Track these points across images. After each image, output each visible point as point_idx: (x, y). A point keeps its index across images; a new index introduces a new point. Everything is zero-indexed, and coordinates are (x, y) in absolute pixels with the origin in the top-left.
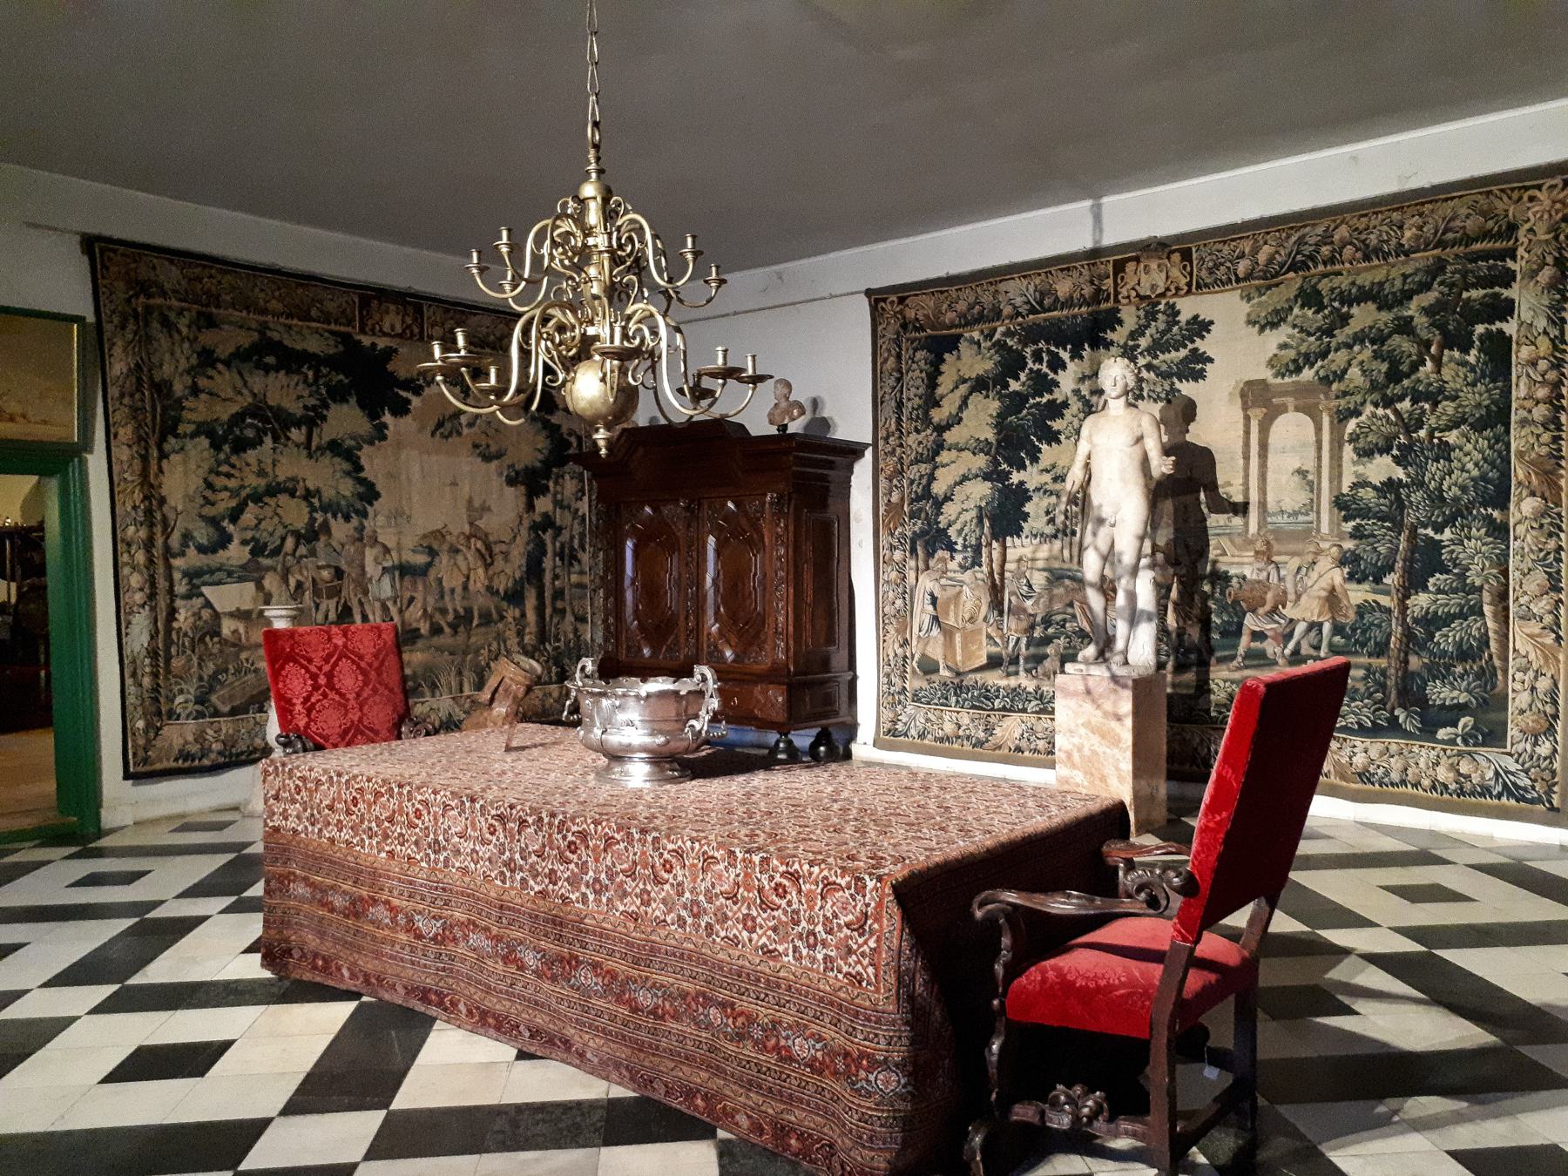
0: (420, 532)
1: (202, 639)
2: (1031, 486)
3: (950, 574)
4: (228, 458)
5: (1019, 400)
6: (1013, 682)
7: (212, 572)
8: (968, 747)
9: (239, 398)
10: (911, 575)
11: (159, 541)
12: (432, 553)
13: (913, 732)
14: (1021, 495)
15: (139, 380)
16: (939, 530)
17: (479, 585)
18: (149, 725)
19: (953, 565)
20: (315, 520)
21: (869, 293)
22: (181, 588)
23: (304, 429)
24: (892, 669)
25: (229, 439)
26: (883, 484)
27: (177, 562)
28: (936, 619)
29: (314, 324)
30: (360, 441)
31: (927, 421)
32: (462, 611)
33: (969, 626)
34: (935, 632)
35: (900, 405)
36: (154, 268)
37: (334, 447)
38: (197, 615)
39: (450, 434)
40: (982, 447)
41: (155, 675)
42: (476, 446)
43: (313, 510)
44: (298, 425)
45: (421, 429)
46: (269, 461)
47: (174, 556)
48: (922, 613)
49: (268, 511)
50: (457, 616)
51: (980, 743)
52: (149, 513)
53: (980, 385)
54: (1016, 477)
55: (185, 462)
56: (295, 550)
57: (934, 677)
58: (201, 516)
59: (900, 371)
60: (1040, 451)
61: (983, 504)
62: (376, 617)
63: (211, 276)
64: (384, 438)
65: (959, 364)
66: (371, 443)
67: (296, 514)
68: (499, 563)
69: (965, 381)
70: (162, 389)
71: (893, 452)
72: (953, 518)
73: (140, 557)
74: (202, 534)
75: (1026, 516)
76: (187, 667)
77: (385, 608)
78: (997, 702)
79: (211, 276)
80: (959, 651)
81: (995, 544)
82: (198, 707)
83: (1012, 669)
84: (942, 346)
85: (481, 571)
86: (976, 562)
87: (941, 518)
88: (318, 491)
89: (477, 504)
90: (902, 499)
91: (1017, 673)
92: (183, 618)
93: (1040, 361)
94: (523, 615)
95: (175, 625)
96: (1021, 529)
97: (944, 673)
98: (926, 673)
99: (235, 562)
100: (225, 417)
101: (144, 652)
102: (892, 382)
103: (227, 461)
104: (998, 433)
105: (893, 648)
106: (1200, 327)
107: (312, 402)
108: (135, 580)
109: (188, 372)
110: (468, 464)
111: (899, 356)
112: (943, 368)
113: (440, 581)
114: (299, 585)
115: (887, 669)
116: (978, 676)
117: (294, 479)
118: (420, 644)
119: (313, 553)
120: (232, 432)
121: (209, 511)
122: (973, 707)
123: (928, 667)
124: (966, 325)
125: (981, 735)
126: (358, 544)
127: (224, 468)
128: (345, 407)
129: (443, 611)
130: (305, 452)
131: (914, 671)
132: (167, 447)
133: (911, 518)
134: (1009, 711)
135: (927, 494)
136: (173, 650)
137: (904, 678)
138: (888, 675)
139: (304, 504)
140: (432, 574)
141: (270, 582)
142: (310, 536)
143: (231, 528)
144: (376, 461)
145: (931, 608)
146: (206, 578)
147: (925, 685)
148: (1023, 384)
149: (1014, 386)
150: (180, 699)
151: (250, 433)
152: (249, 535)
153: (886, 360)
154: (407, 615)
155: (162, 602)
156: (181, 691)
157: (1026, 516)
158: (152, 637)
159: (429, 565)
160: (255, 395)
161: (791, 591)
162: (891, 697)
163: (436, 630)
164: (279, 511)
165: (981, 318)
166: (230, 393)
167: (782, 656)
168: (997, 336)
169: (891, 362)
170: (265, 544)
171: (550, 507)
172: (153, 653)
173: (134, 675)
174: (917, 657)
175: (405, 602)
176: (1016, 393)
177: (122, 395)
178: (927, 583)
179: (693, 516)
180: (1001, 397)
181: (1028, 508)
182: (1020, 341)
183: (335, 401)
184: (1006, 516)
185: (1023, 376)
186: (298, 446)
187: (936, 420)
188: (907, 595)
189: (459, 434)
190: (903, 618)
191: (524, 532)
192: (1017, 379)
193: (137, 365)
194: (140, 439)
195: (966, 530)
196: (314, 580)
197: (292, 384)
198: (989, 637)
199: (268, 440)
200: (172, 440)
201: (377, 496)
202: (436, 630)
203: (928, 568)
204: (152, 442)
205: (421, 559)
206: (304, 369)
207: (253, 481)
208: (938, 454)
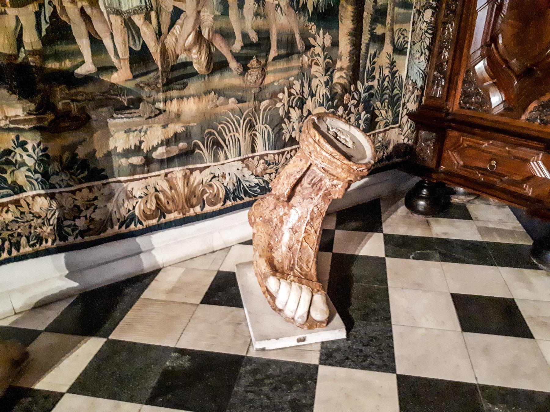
32: (254, 37)
50: (247, 44)
94: (335, 44)
118: (194, 86)
129: (227, 35)
154: (170, 41)
175: (166, 19)
202: (218, 65)
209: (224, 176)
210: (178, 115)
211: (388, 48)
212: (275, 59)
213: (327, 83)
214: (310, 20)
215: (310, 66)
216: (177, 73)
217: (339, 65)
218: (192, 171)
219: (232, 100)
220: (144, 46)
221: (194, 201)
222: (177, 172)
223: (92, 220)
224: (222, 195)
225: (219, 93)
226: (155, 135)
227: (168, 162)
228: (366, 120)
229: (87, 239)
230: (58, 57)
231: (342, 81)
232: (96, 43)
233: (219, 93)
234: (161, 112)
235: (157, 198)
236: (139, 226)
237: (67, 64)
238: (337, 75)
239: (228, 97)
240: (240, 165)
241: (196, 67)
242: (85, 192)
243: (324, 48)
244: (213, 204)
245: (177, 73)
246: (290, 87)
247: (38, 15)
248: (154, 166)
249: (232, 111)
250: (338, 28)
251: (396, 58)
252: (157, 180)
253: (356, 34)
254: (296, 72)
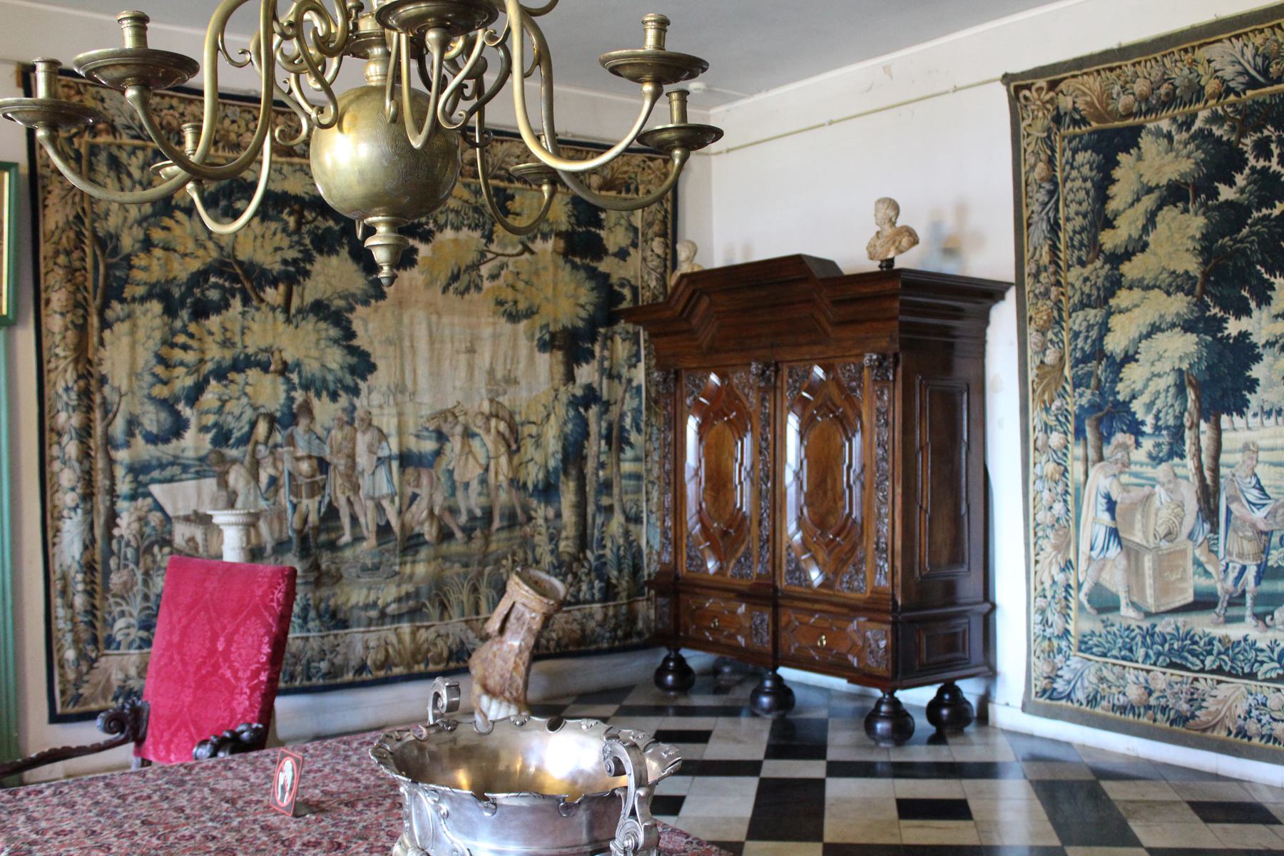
0: (426, 411)
1: (148, 550)
2: (1259, 338)
3: (1133, 468)
4: (185, 326)
5: (1233, 215)
6: (1234, 632)
7: (162, 466)
8: (1162, 722)
9: (201, 252)
10: (1077, 470)
11: (98, 429)
12: (441, 437)
13: (1080, 695)
14: (1245, 351)
15: (79, 235)
16: (1117, 404)
17: (501, 478)
18: (81, 655)
19: (1139, 455)
20: (291, 400)
21: (1007, 79)
22: (124, 487)
23: (282, 288)
24: (1051, 602)
25: (188, 302)
26: (1033, 338)
27: (122, 455)
28: (1114, 533)
29: (296, 160)
30: (353, 301)
31: (1095, 247)
32: (478, 513)
33: (1164, 544)
34: (1114, 551)
35: (1054, 228)
36: (102, 100)
37: (319, 309)
38: (142, 520)
39: (467, 289)
40: (1179, 283)
41: (90, 593)
42: (500, 303)
43: (291, 387)
44: (274, 283)
45: (430, 284)
46: (237, 329)
47: (116, 447)
48: (1094, 523)
49: (234, 390)
50: (472, 518)
51: (1182, 719)
52: (85, 394)
53: (1175, 194)
54: (1234, 327)
55: (133, 332)
56: (268, 438)
57: (1111, 617)
58: (150, 397)
59: (1053, 180)
60: (1271, 287)
61: (1185, 366)
62: (368, 521)
63: (172, 107)
64: (381, 295)
65: (1142, 167)
66: (366, 303)
67: (269, 392)
68: (529, 449)
69: (1150, 190)
70: (107, 244)
71: (1046, 294)
72: (1138, 386)
73: (72, 448)
74: (152, 419)
75: (1252, 384)
76: (128, 586)
77: (380, 508)
78: (1209, 660)
79: (172, 107)
80: (1149, 581)
81: (1204, 426)
82: (143, 634)
83: (1234, 611)
84: (1113, 143)
85: (504, 460)
86: (1176, 451)
87: (1120, 387)
88: (298, 365)
89: (499, 374)
90: (1062, 359)
91: (1241, 619)
92: (126, 525)
93: (1268, 156)
94: (558, 515)
95: (116, 532)
96: (1246, 403)
97: (1127, 612)
98: (1101, 610)
99: (190, 454)
100: (183, 276)
101: (76, 566)
102: (1042, 196)
103: (184, 330)
104: (1205, 263)
105: (1050, 571)
107: (292, 254)
108: (67, 477)
109: (140, 223)
110: (490, 326)
111: (1051, 161)
112: (1117, 173)
113: (451, 472)
114: (273, 481)
115: (1041, 602)
116: (1180, 619)
117: (269, 350)
118: (424, 553)
119: (291, 441)
120: (192, 294)
121: (161, 391)
122: (1172, 665)
123: (1104, 604)
124: (1149, 111)
125: (1185, 707)
126: (347, 429)
127: (181, 339)
128: (334, 260)
130: (281, 317)
131: (1081, 608)
132: (110, 314)
133: (1075, 386)
134: (1229, 674)
135: (1098, 353)
136: (113, 563)
137: (1066, 617)
138: (1043, 611)
139: (280, 380)
140: (443, 464)
141: (237, 478)
142: (286, 419)
143: (187, 412)
144: (371, 326)
145: (1106, 517)
146: (156, 474)
147: (1099, 628)
148: (1242, 191)
149: (1226, 193)
150: (120, 623)
151: (214, 295)
152: (210, 420)
153: (1033, 167)
154: (408, 516)
155: (101, 502)
156: (122, 614)
157: (1252, 384)
158: (86, 547)
159: (438, 453)
160: (221, 248)
161: (899, 490)
162: (1048, 644)
163: (445, 535)
164: (249, 389)
165: (1170, 101)
166: (191, 246)
167: (885, 583)
168: (1198, 124)
169: (1041, 170)
170: (230, 432)
171: (597, 377)
172: (89, 567)
173: (64, 593)
174: (1085, 589)
175: (407, 501)
176: (1228, 203)
177: (57, 253)
178: (1100, 481)
179: (769, 388)
180: (1207, 211)
181: (1257, 371)
182: (1233, 129)
183: (321, 252)
185: (1240, 180)
186: (273, 309)
187: (1108, 246)
188: (1072, 497)
189: (479, 288)
190: (1066, 530)
191: (561, 410)
192: (1231, 183)
193: (78, 217)
194: (77, 305)
195: (1159, 404)
196: (290, 474)
197: (268, 234)
198: (1198, 563)
199: (237, 303)
200: (116, 305)
201: (372, 368)
203: (1101, 459)
204: (93, 310)
205: (429, 446)
206: (285, 216)
207: (215, 353)
208: (1113, 295)
209: (447, 636)
210: (411, 577)
211: (618, 519)
212: (498, 530)
213: (552, 552)
214: (531, 495)
215: (533, 536)
216: (412, 542)
217: (564, 534)
218: (419, 628)
219: (457, 566)
220: (388, 523)
221: (419, 657)
222: (406, 627)
223: (333, 664)
224: (445, 654)
225: (445, 558)
226: (388, 594)
227: (398, 618)
228: (601, 589)
229: (328, 682)
230: (328, 530)
231: (570, 550)
232: (354, 520)
233: (445, 558)
234: (396, 573)
235: (387, 651)
236: (370, 676)
237: (333, 536)
238: (562, 545)
239: (453, 563)
240: (464, 626)
241: (427, 537)
242: (331, 638)
243: (546, 520)
244: (437, 663)
245: (412, 542)
246: (514, 554)
247: (320, 503)
248: (388, 620)
249: (458, 575)
250: (560, 502)
251: (632, 527)
252: (387, 632)
253: (581, 506)
254: (518, 541)
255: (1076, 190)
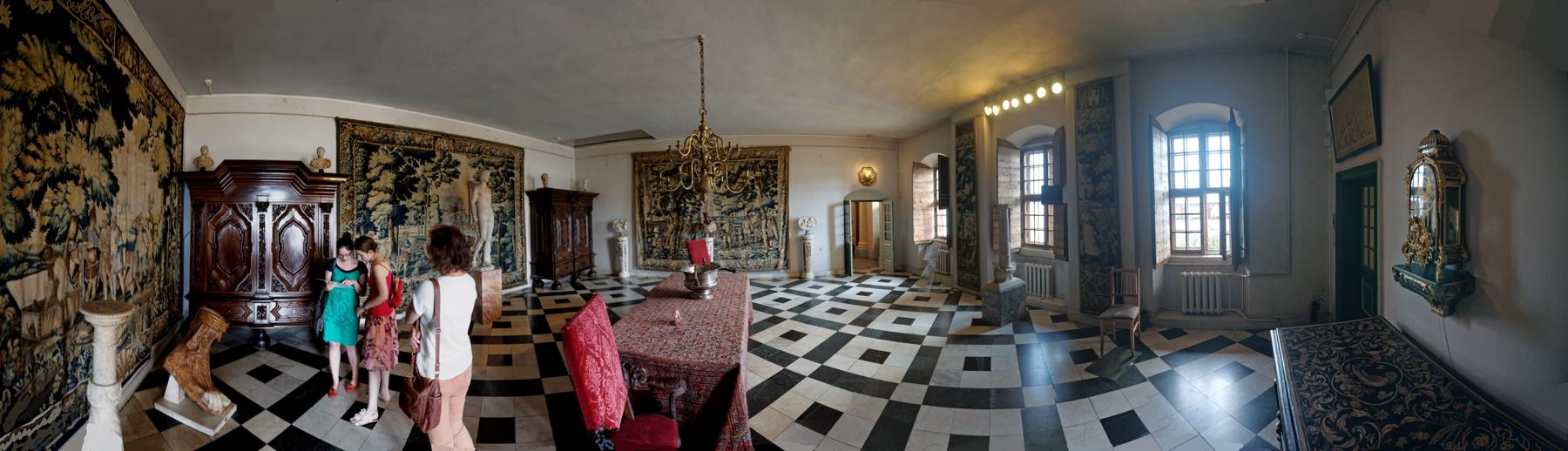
14: (404, 209)
31: (364, 177)
53: (387, 167)
84: (370, 149)
106: (457, 163)
135: (364, 207)
165: (387, 142)
184: (398, 217)
255: (359, 159)
